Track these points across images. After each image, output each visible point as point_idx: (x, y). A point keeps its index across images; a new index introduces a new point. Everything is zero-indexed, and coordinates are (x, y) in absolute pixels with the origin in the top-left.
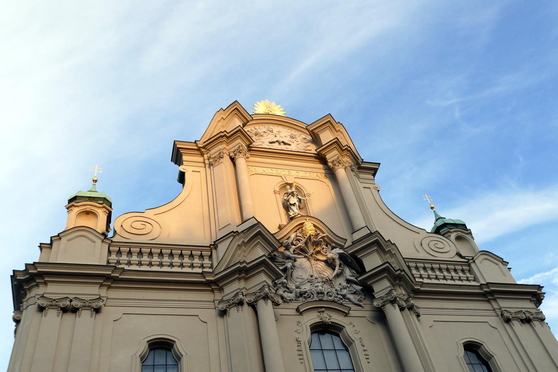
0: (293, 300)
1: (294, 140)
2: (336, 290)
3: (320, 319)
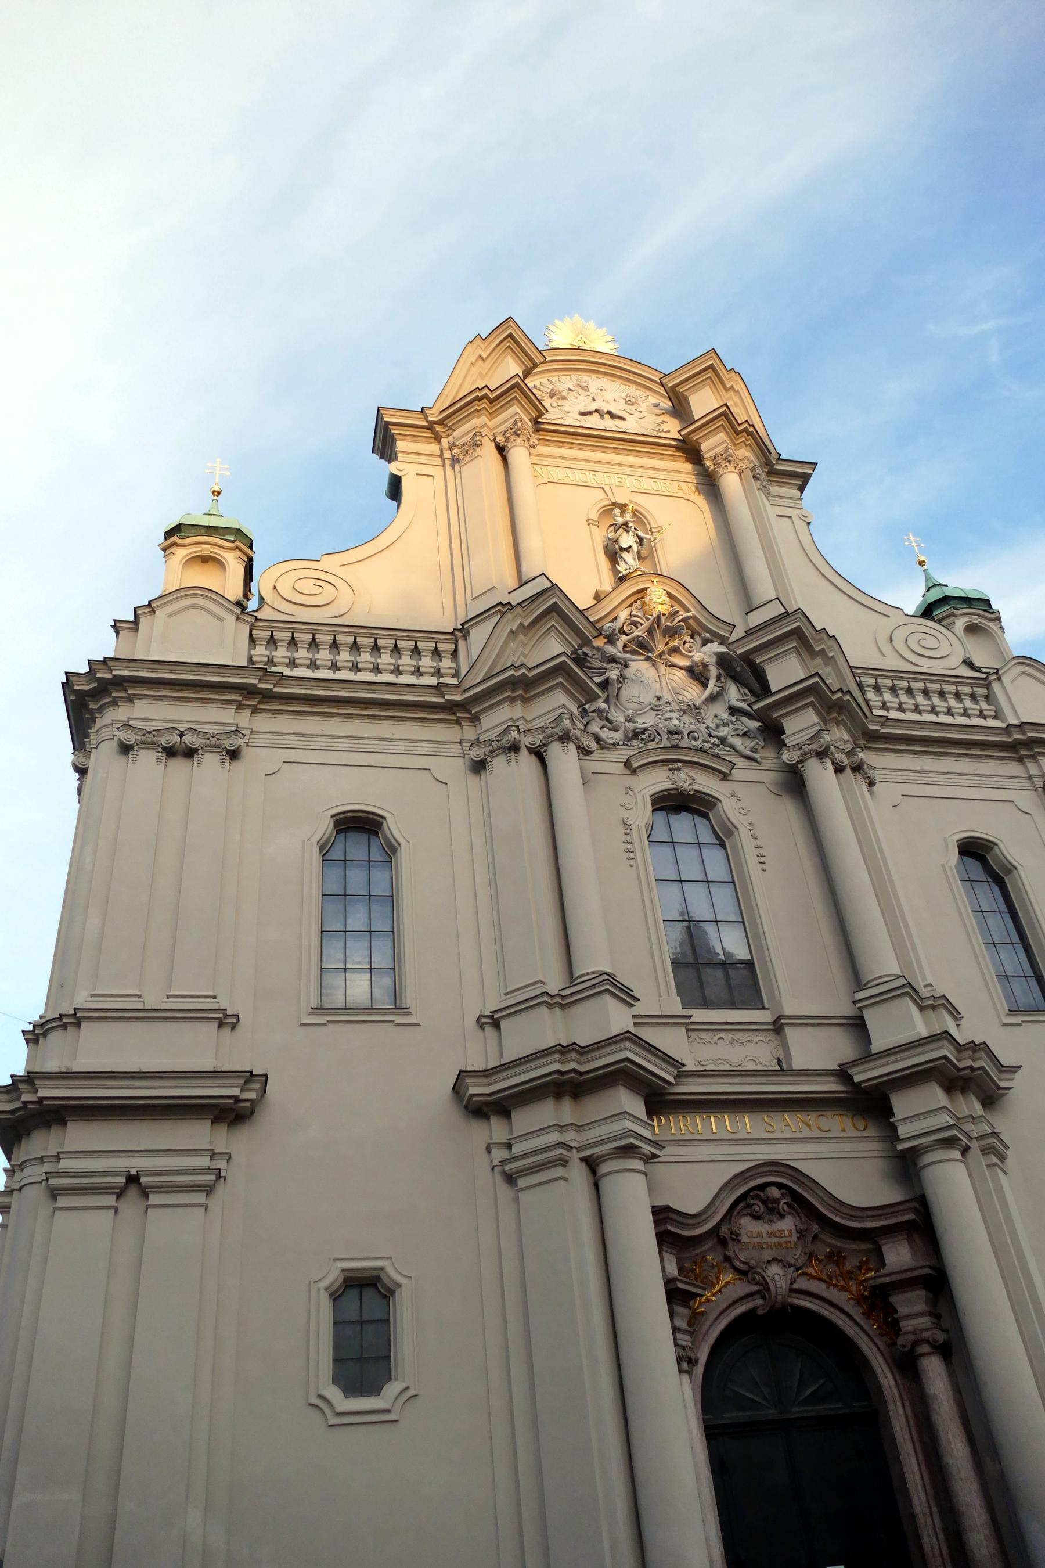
0: (618, 745)
1: (632, 407)
2: (707, 727)
3: (673, 784)
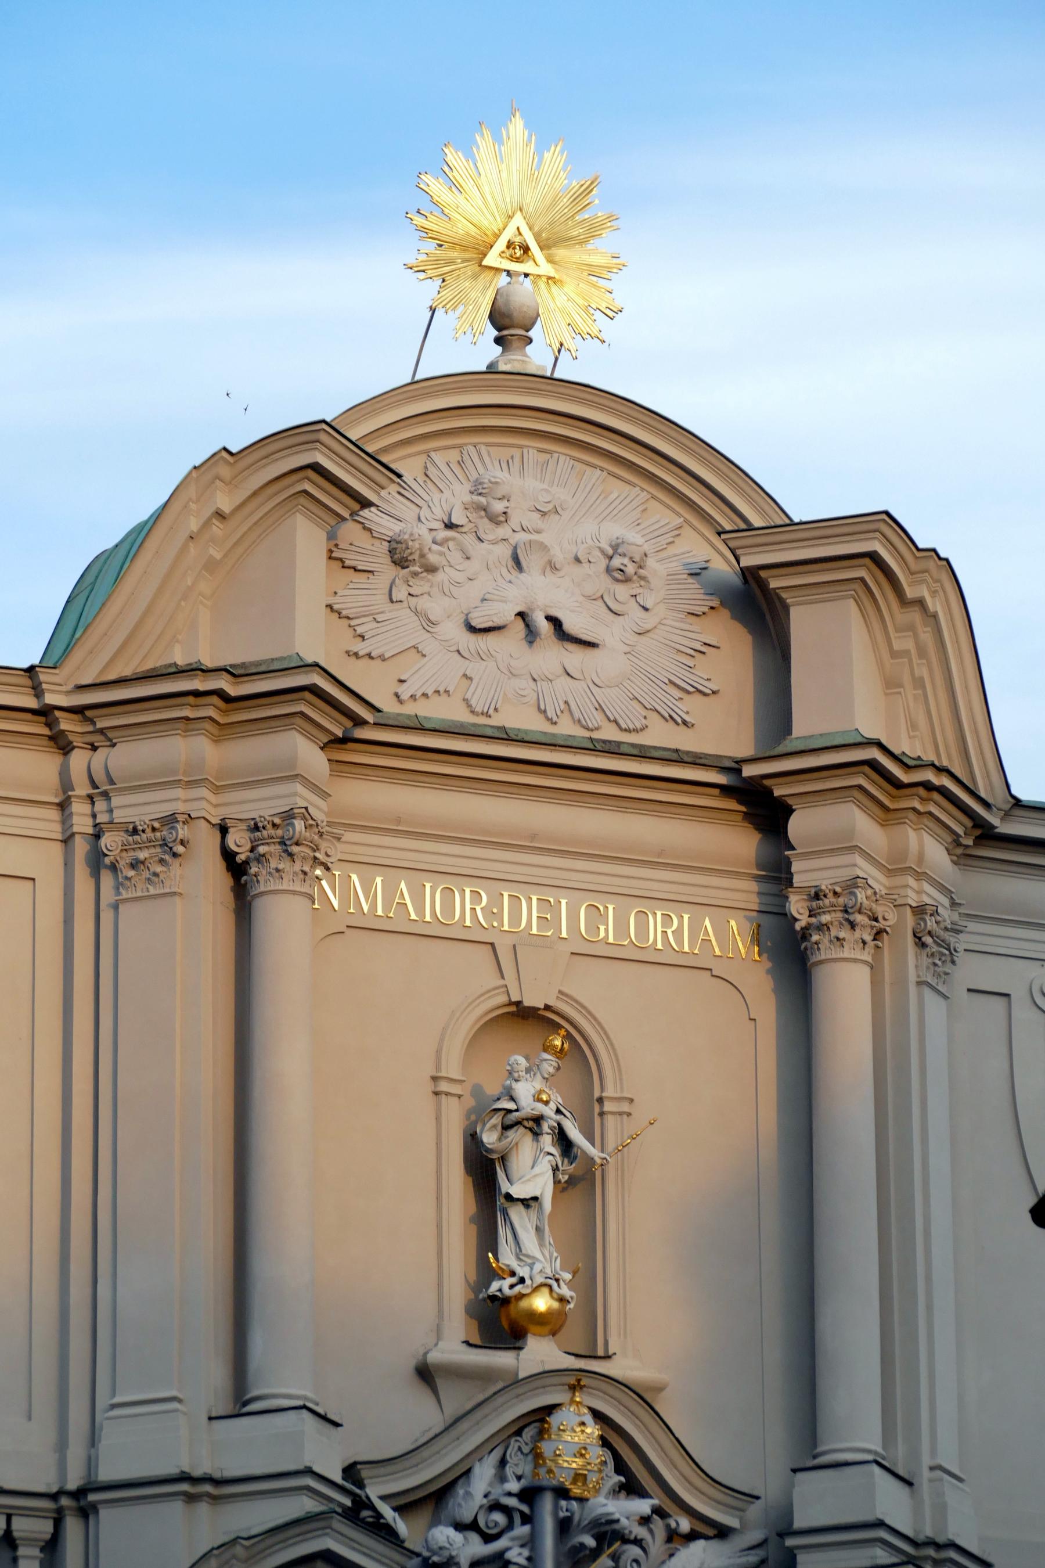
1: (622, 591)
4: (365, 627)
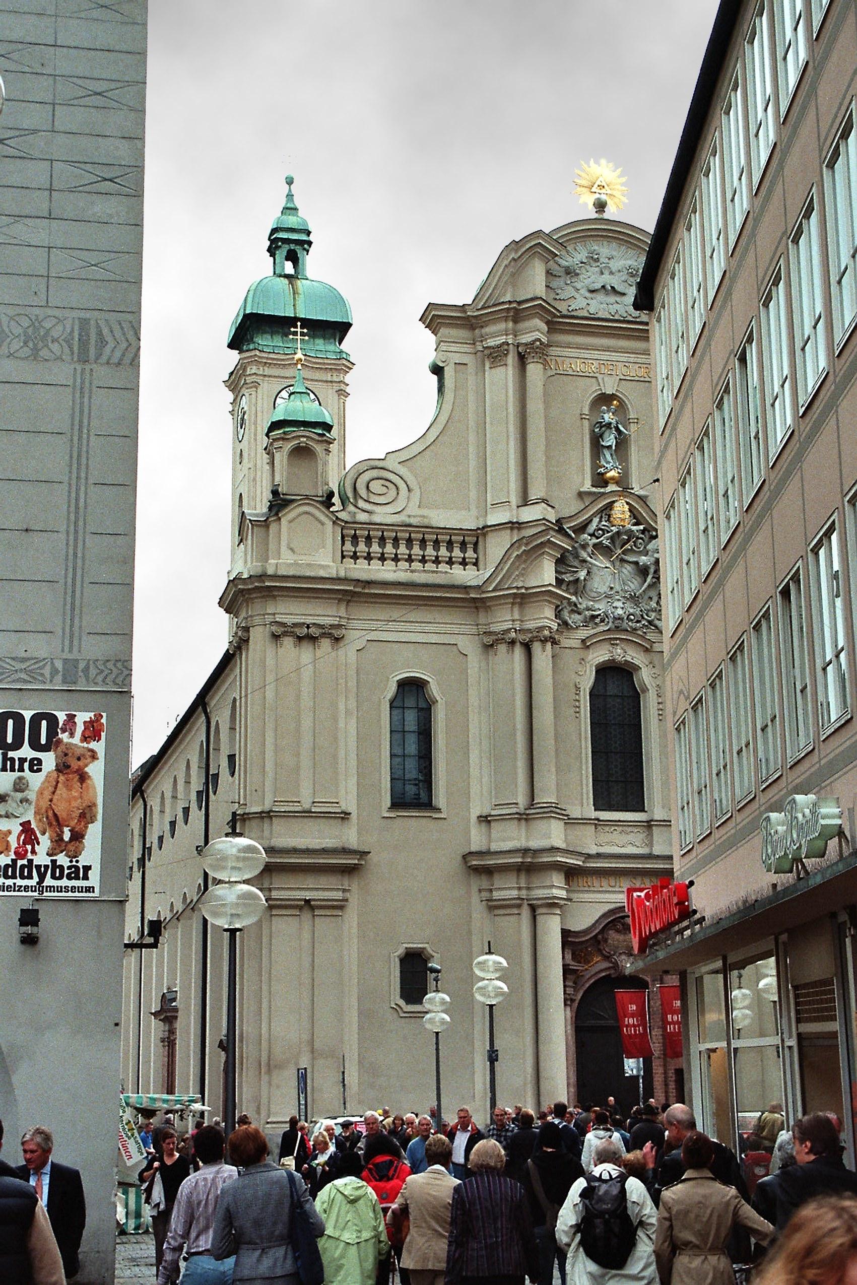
4: (559, 291)
